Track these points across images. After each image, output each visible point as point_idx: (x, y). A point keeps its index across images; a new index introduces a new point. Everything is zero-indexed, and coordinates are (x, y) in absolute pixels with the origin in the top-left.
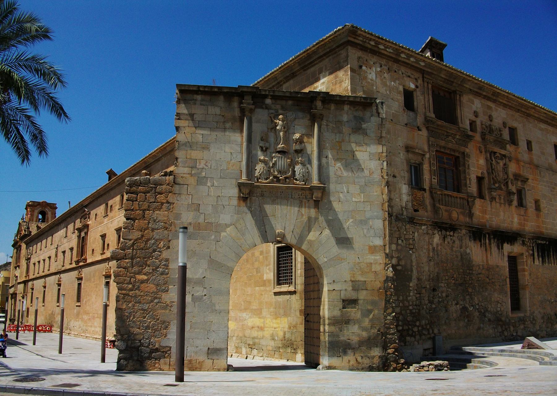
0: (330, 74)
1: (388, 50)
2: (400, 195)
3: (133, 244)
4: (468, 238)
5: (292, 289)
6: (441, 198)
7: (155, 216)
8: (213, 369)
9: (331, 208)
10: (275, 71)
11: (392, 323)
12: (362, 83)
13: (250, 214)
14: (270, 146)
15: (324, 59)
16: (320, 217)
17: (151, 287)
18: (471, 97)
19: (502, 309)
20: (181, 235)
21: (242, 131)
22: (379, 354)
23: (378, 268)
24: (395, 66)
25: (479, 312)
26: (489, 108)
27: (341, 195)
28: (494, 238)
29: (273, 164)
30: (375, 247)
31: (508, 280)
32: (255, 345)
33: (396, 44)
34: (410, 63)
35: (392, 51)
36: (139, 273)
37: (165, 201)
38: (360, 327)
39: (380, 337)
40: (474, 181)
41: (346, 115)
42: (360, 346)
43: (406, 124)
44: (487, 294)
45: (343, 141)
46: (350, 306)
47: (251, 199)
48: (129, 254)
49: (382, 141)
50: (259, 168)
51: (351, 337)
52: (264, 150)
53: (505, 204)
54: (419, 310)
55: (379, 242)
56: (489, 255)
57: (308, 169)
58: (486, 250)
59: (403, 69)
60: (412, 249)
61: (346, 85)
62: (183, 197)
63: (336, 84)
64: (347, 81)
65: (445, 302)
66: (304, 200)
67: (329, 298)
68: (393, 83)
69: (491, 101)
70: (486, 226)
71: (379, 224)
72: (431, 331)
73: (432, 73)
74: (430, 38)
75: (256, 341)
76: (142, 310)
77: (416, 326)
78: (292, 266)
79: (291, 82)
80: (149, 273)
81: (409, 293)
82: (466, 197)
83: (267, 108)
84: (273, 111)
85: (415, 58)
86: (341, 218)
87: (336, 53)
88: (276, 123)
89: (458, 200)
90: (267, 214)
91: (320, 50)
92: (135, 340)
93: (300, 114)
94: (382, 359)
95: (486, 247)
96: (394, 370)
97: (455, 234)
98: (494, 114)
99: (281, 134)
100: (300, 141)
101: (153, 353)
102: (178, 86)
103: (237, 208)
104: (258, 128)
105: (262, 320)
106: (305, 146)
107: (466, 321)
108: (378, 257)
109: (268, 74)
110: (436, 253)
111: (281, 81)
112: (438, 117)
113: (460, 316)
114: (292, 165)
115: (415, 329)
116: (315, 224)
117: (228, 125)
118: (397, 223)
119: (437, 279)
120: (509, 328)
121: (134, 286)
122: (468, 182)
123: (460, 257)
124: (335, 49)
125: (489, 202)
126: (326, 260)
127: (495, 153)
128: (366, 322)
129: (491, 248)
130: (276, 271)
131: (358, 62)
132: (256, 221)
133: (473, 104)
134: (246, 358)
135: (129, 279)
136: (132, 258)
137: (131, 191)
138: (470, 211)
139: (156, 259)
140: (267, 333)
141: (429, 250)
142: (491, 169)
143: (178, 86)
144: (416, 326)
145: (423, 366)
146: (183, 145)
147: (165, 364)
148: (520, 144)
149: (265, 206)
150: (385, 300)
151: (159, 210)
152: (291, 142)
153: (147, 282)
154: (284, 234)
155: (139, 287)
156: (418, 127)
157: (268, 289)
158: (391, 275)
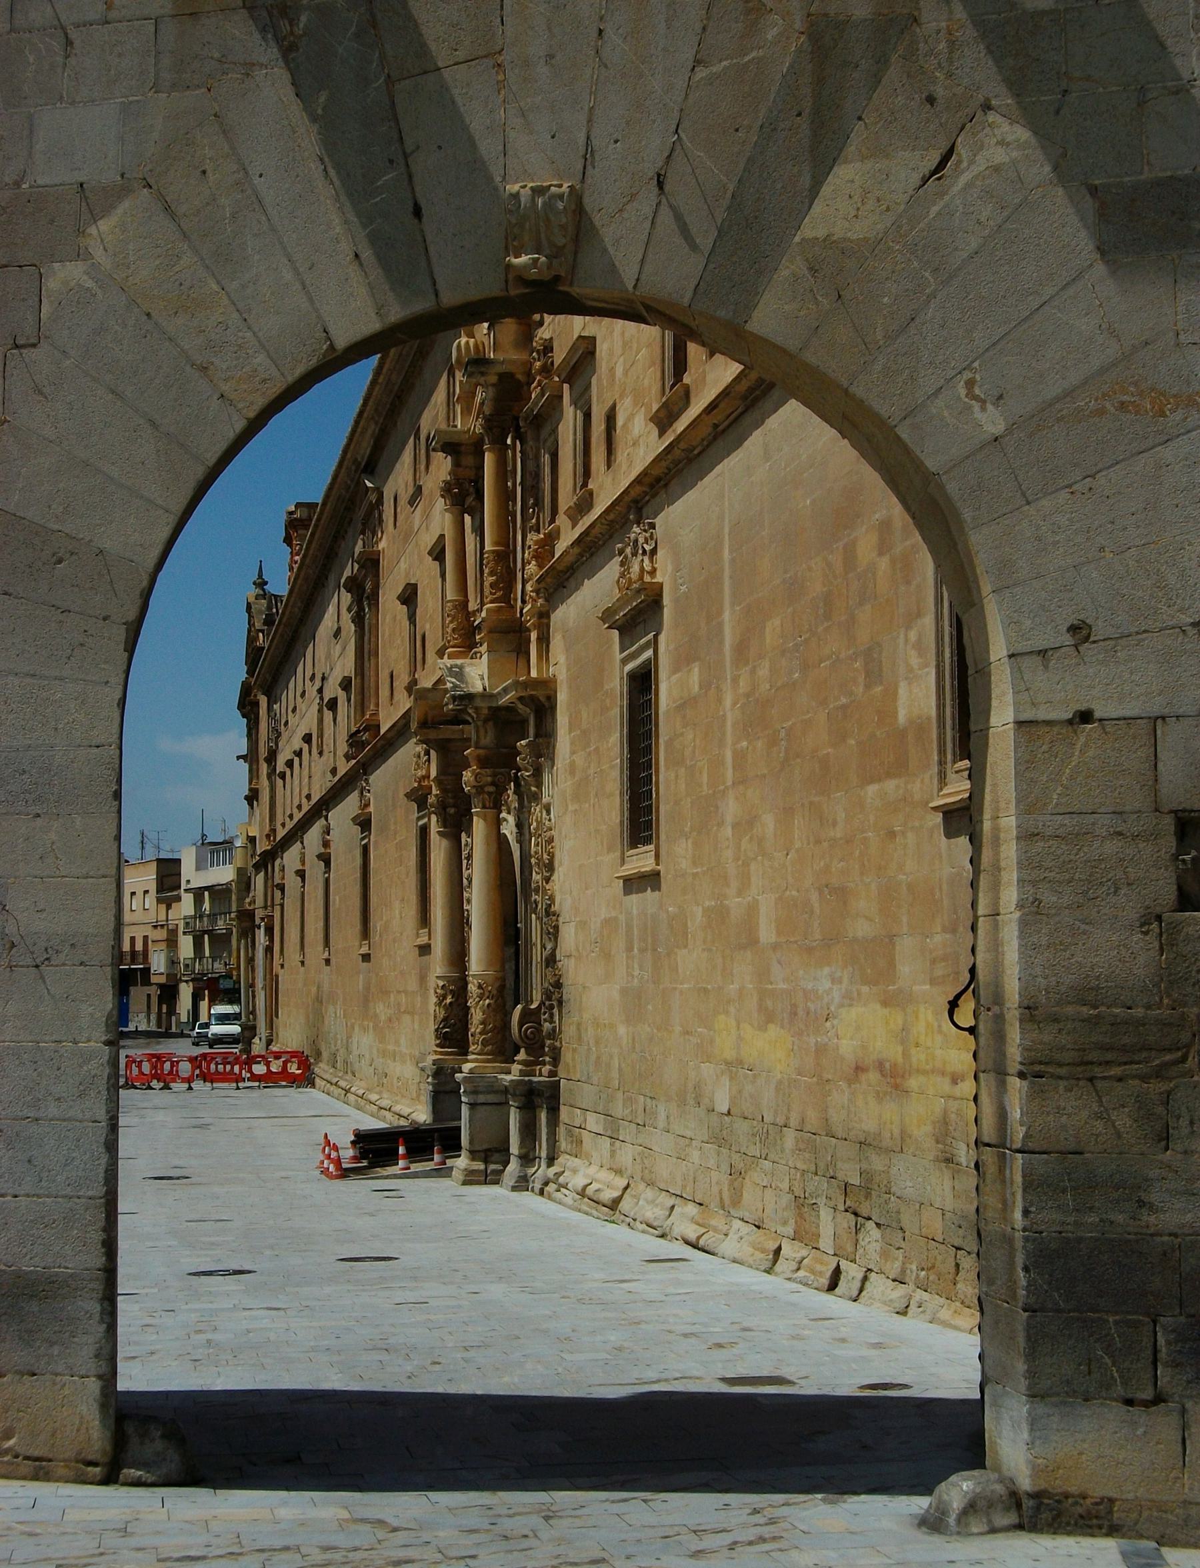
13: (281, 73)
67: (1027, 805)
90: (423, 51)
116: (876, 80)
126: (992, 421)
132: (328, 125)
154: (578, 210)
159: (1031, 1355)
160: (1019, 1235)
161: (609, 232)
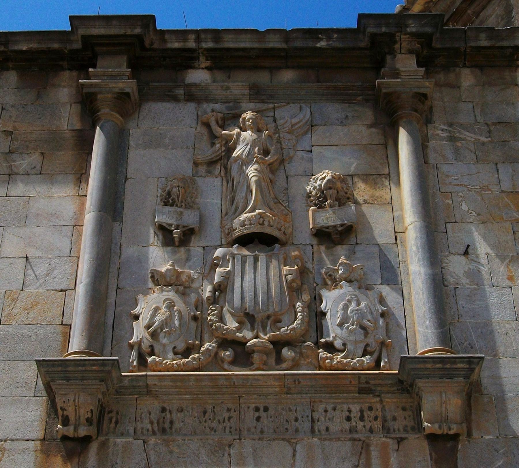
14: (202, 220)
21: (81, 176)
29: (215, 290)
47: (104, 445)
50: (151, 306)
52: (177, 239)
57: (382, 301)
66: (378, 440)
83: (190, 98)
93: (334, 110)
99: (252, 171)
100: (337, 194)
106: (361, 215)
114: (306, 285)
117: (23, 163)
152: (299, 204)
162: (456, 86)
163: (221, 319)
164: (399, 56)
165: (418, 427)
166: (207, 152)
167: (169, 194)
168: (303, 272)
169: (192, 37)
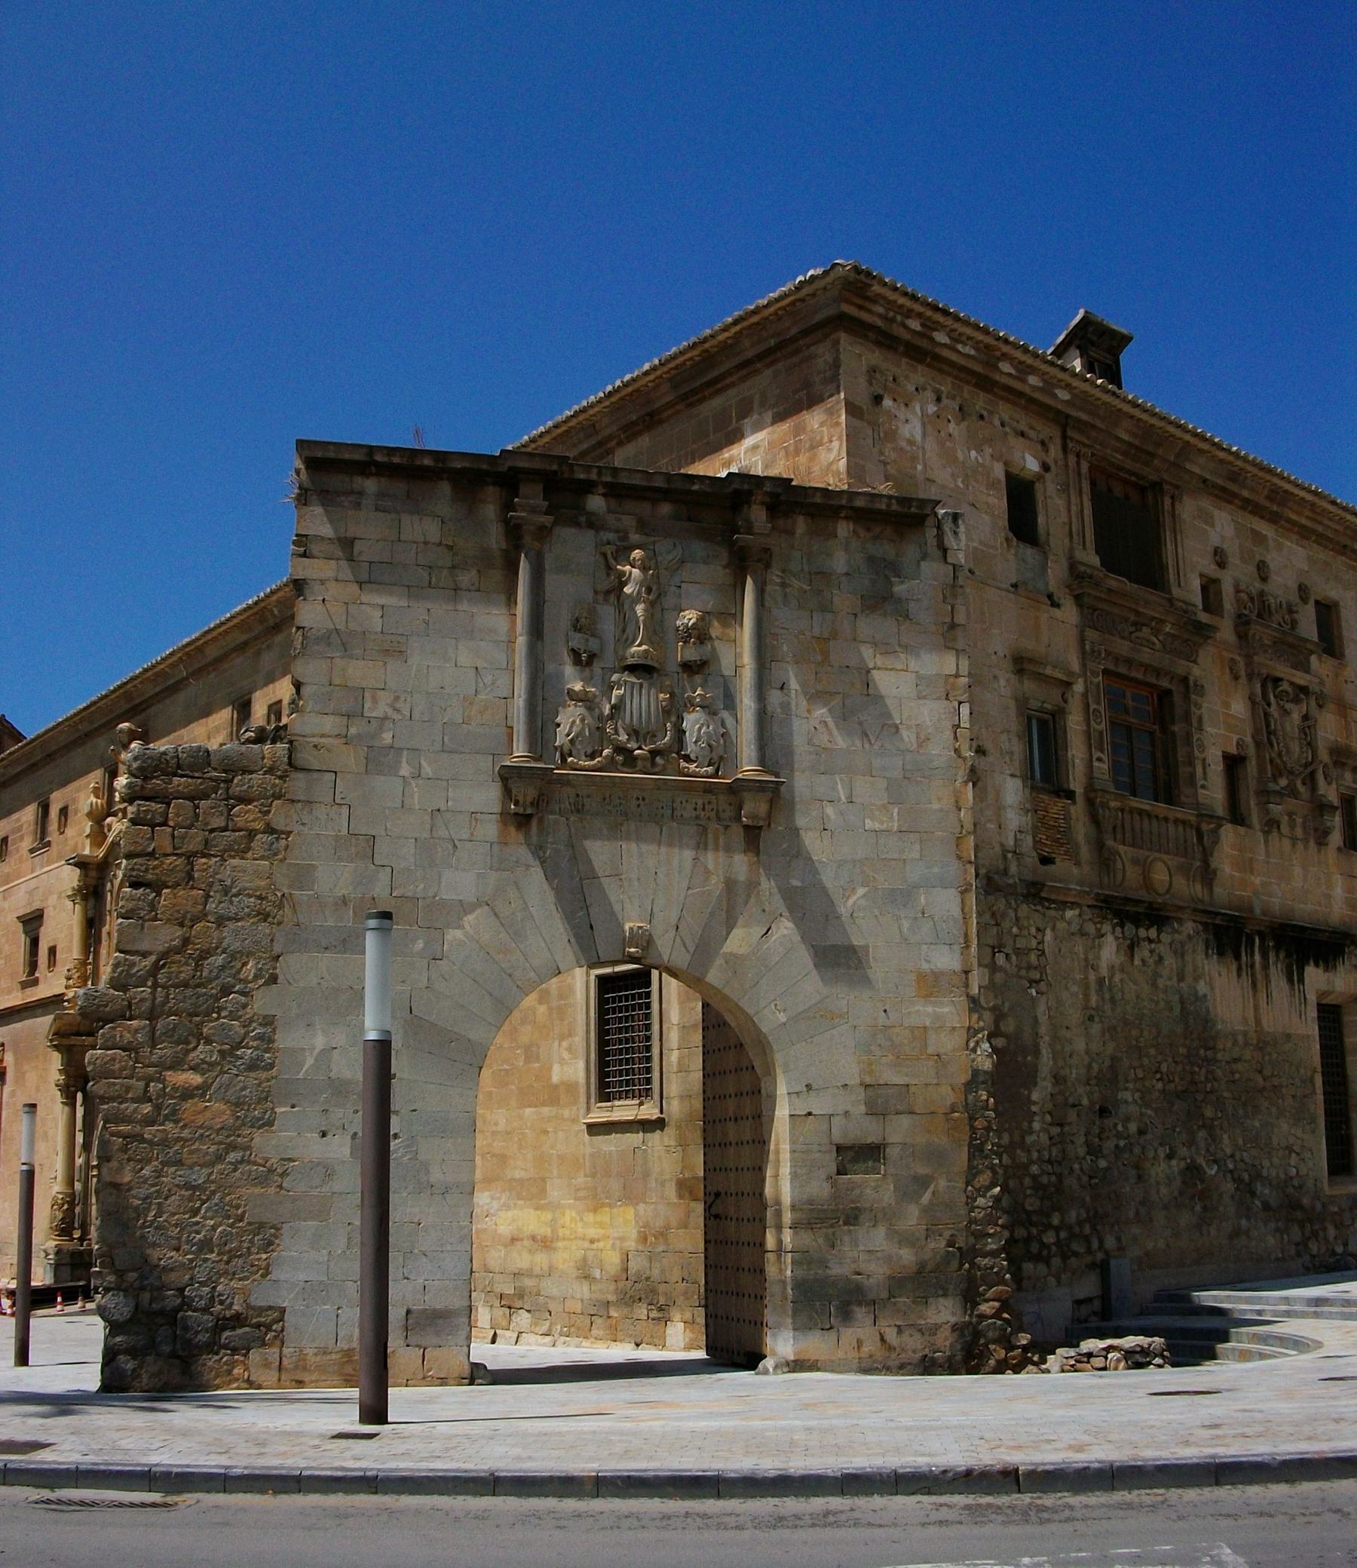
0: (779, 418)
1: (960, 347)
2: (1000, 809)
3: (156, 968)
4: (1201, 947)
5: (649, 1111)
6: (1119, 823)
7: (226, 875)
8: (426, 1380)
9: (797, 852)
10: (591, 406)
11: (991, 1220)
12: (882, 453)
13: (539, 870)
15: (757, 372)
16: (763, 879)
17: (217, 1111)
18: (1206, 503)
19: (1304, 1170)
20: (371, 941)
21: (511, 599)
22: (953, 1320)
23: (948, 1043)
24: (980, 401)
25: (1234, 1180)
26: (1258, 538)
27: (829, 810)
28: (1277, 949)
29: (613, 707)
30: (937, 975)
31: (1319, 1080)
32: (521, 1296)
33: (985, 331)
34: (1027, 390)
35: (973, 352)
36: (176, 1065)
37: (259, 825)
38: (891, 1233)
39: (955, 1264)
40: (1217, 768)
41: (843, 551)
42: (891, 1296)
43: (1015, 586)
44: (1257, 1124)
45: (834, 635)
46: (862, 1166)
47: (541, 821)
48: (142, 1000)
49: (954, 639)
50: (569, 720)
51: (863, 1267)
52: (583, 660)
53: (1306, 840)
54: (1060, 1176)
55: (947, 960)
56: (1263, 1003)
57: (723, 725)
58: (1254, 985)
59: (1005, 411)
60: (1037, 982)
61: (832, 457)
62: (320, 812)
63: (797, 452)
64: (836, 444)
65: (1137, 1150)
66: (713, 826)
67: (793, 1142)
68: (973, 453)
69: (1262, 517)
70: (1251, 909)
71: (948, 904)
72: (1095, 1245)
73: (1093, 426)
74: (1081, 313)
75: (528, 1283)
76: (187, 1186)
77: (1049, 1226)
78: (648, 1038)
79: (644, 441)
80: (210, 1064)
81: (1031, 1122)
82: (1193, 819)
83: (591, 525)
84: (611, 536)
85: (1043, 375)
86: (828, 885)
87: (797, 352)
88: (623, 573)
89: (1172, 828)
90: (593, 870)
91: (747, 343)
92: (163, 1287)
93: (698, 548)
94: (962, 1335)
95: (1253, 975)
96: (1000, 1369)
97: (1163, 936)
98: (1273, 560)
99: (640, 609)
100: (699, 634)
101: (224, 1329)
102: (301, 444)
103: (496, 847)
104: (567, 590)
105: (547, 1216)
106: (714, 649)
107: (1198, 1208)
108: (946, 1010)
109: (569, 413)
110: (1107, 996)
111: (610, 438)
112: (1110, 564)
113: (1181, 1194)
114: (674, 711)
115: (1049, 1238)
116: (746, 902)
117: (466, 578)
118: (991, 898)
119: (1110, 1078)
120: (1325, 1229)
121: (158, 1108)
122: (1199, 770)
123: (1177, 1010)
124: (793, 340)
125: (1260, 836)
126: (782, 1018)
127: (1277, 681)
128: (912, 1218)
129: (1267, 977)
130: (593, 1056)
131: (870, 384)
132: (558, 892)
133: (1213, 526)
134: (493, 1342)
135: (142, 1084)
136: (152, 1016)
137: (146, 793)
138: (1206, 863)
139: (232, 1016)
140: (565, 1258)
141: (1087, 987)
142: (1266, 732)
143: (301, 444)
144: (1049, 1226)
145: (1090, 1355)
146: (319, 640)
147: (267, 1365)
148: (1347, 651)
149: (588, 844)
150: (970, 1145)
151: (242, 854)
152: (671, 635)
153: (203, 1095)
155: (174, 1112)
156: (1050, 596)
157: (566, 1113)
158: (987, 1065)
159: (794, 1316)
160: (789, 1280)
161: (659, 943)
162: (791, 533)
163: (617, 733)
164: (754, 507)
165: (738, 818)
166: (605, 584)
167: (577, 620)
168: (672, 695)
169: (595, 471)
